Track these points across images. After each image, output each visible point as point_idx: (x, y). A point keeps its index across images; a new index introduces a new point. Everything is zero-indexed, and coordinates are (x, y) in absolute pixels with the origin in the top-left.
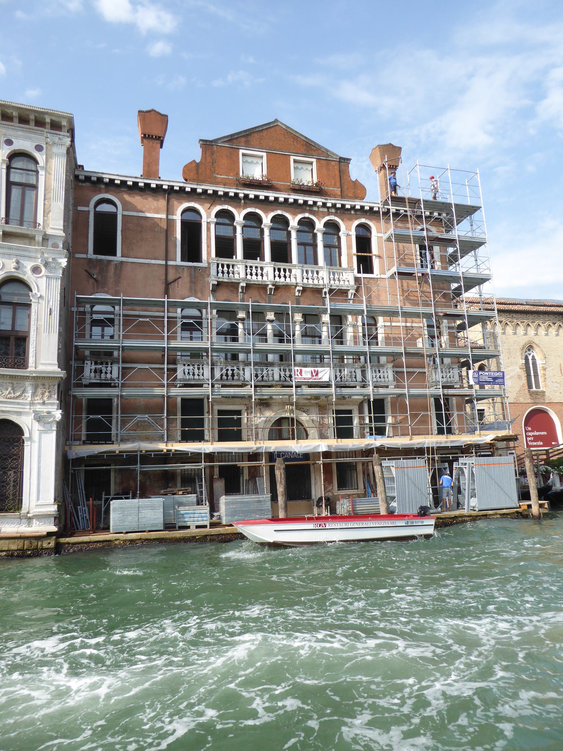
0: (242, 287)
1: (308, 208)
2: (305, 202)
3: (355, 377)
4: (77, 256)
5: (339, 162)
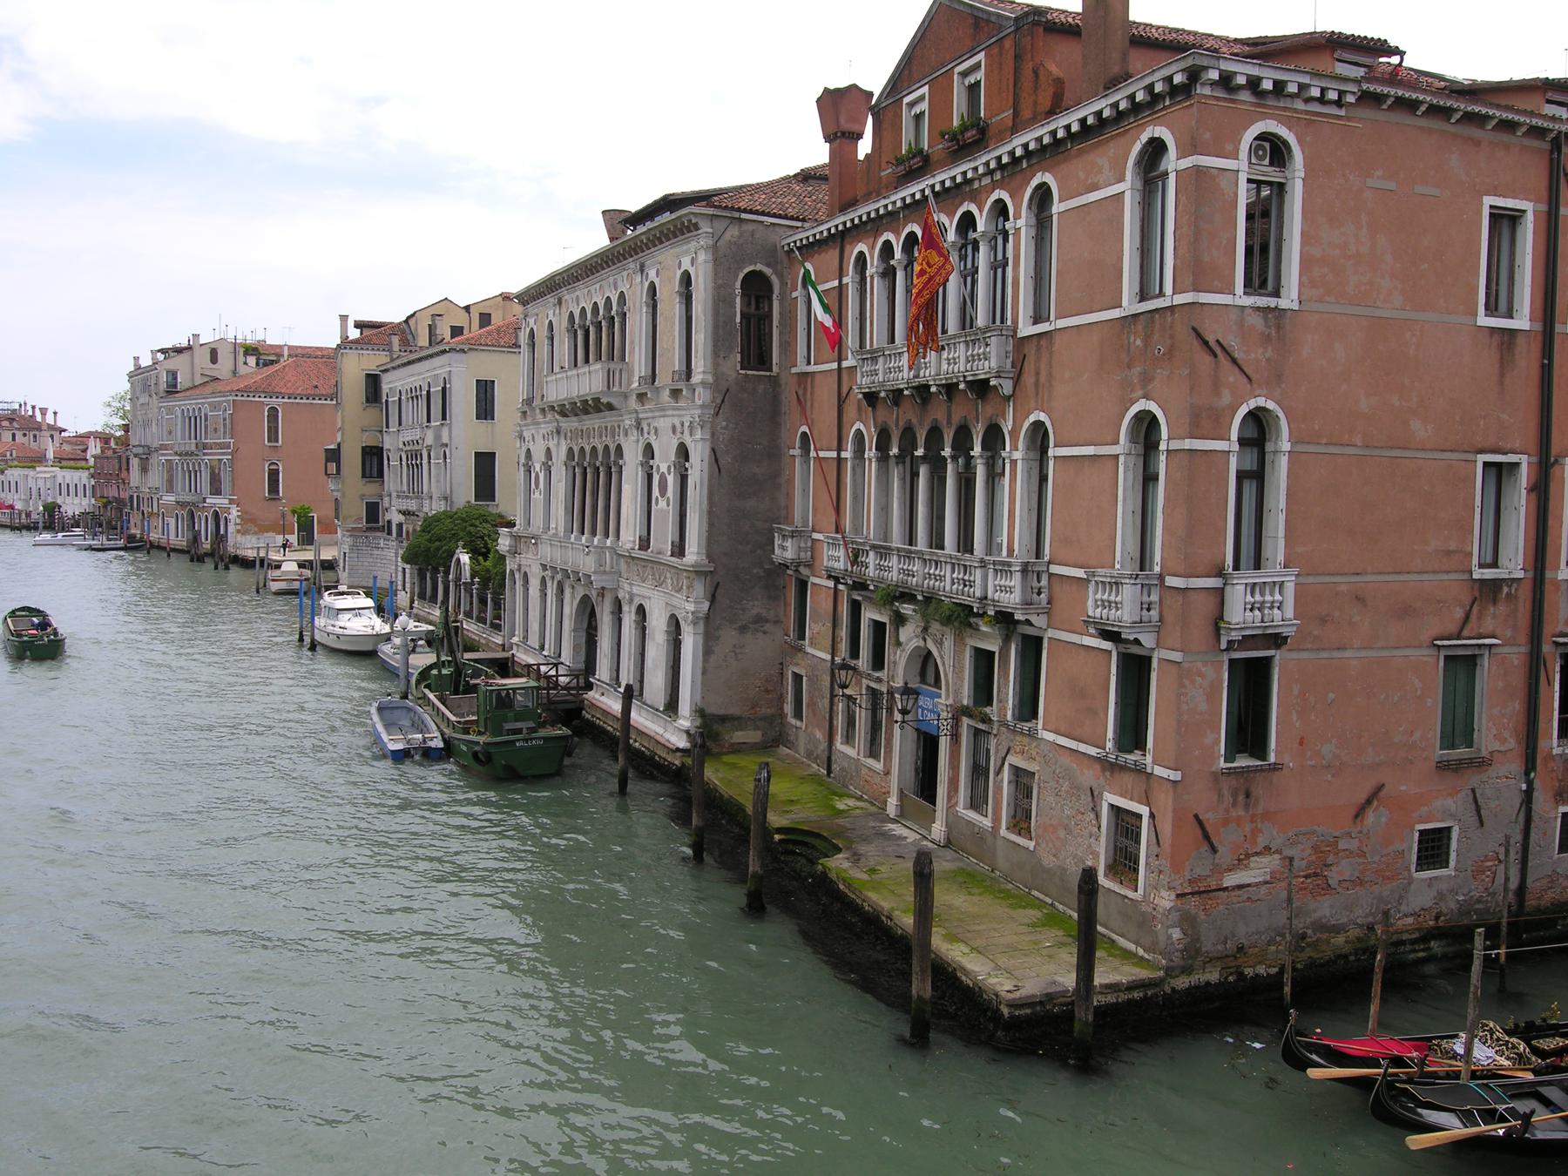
5: (1017, 30)
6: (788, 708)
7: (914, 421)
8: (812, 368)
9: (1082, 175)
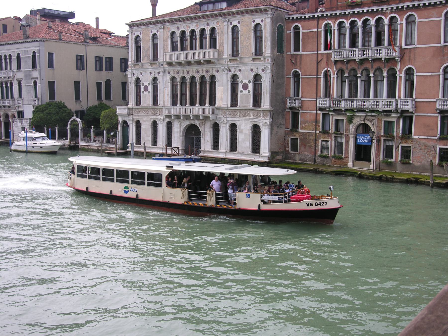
4: (288, 53)
6: (289, 149)
7: (356, 67)
8: (300, 53)
9: (426, 14)
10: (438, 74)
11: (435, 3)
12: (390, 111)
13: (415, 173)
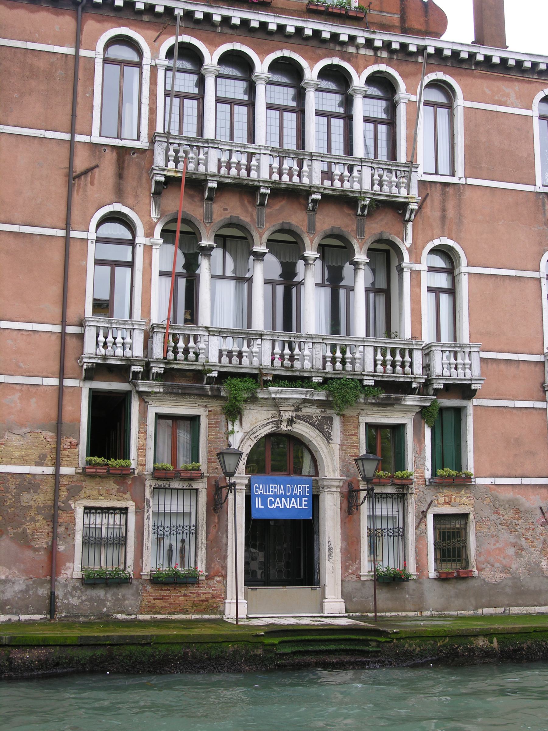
0: (211, 189)
1: (338, 48)
2: (335, 37)
3: (411, 366)
7: (245, 218)
10: (535, 275)
11: (519, 63)
12: (405, 388)
13: (491, 611)
